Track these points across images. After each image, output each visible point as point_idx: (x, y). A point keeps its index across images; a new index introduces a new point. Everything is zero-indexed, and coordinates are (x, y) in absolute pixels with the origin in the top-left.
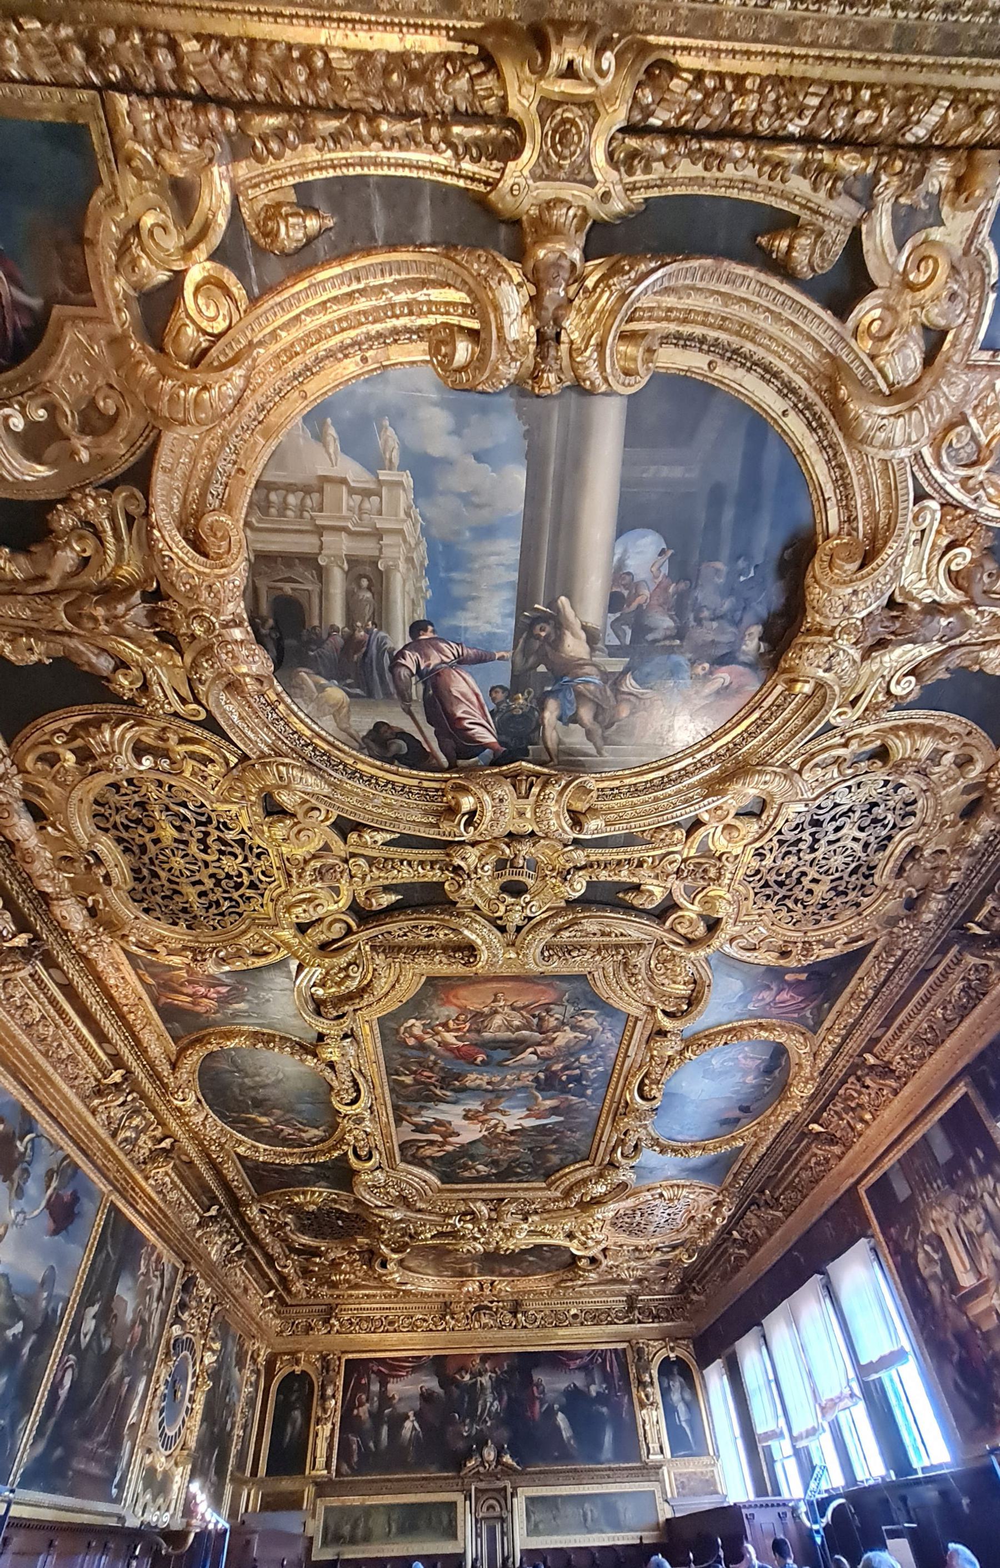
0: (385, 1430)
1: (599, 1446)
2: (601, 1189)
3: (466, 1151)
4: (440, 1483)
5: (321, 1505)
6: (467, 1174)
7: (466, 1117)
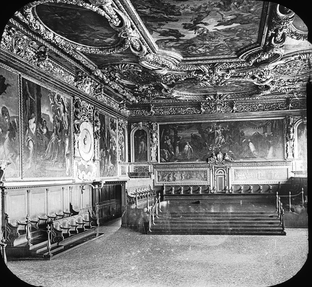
2: (266, 57)
3: (190, 42)
6: (194, 53)
7: (185, 28)
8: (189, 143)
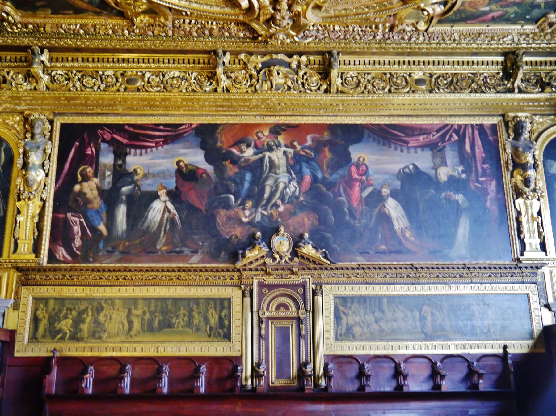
0: (122, 212)
1: (450, 238)
4: (204, 275)
5: (28, 296)
8: (170, 194)
